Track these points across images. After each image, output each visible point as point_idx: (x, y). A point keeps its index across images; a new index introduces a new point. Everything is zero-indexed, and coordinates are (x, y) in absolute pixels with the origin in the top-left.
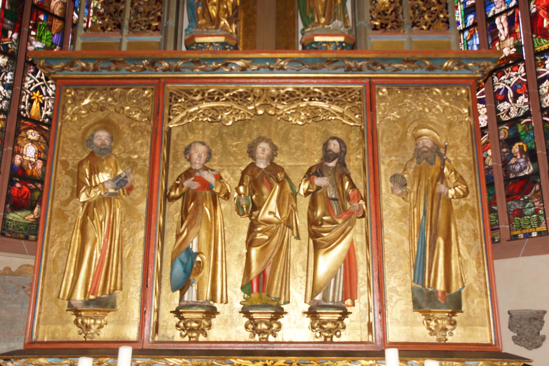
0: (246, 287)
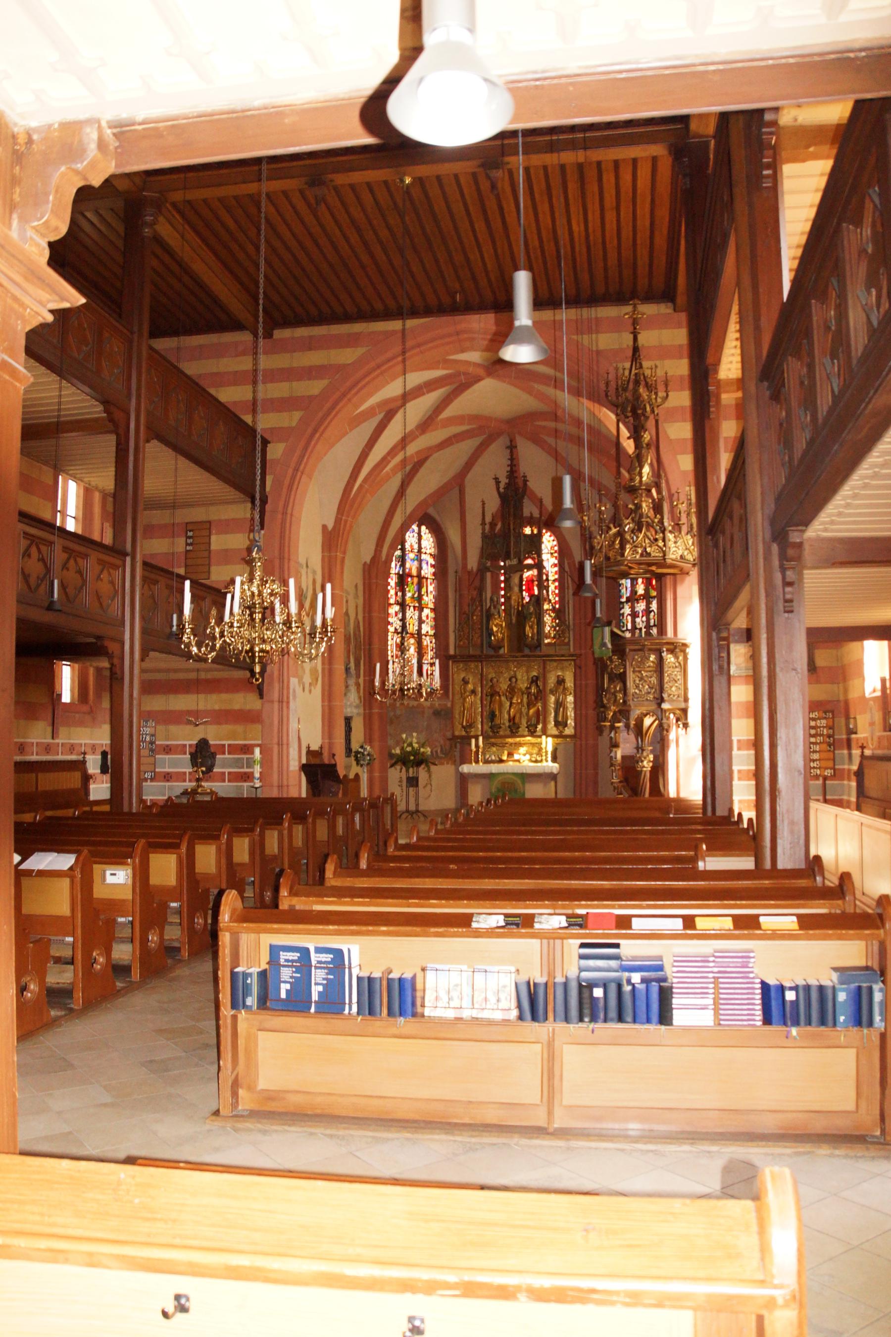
0: (510, 721)
